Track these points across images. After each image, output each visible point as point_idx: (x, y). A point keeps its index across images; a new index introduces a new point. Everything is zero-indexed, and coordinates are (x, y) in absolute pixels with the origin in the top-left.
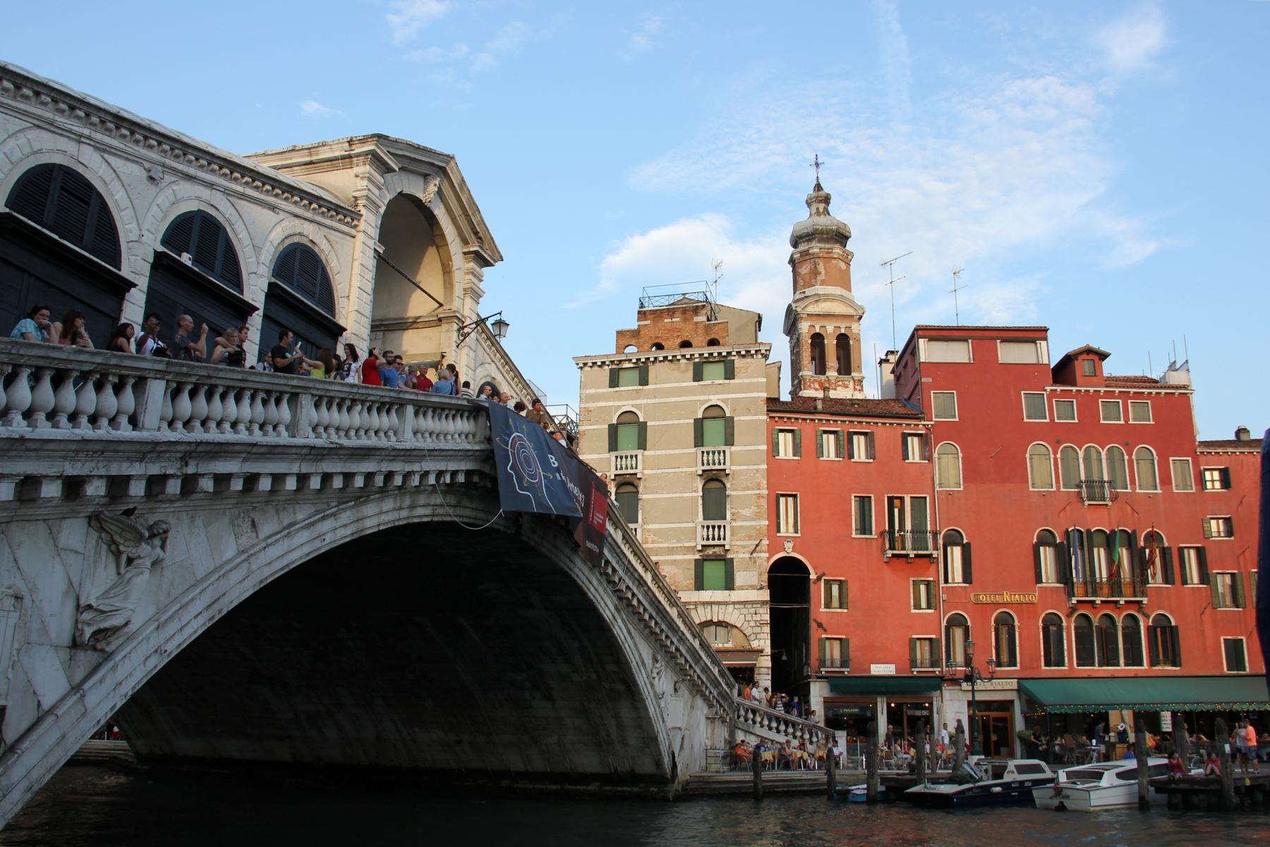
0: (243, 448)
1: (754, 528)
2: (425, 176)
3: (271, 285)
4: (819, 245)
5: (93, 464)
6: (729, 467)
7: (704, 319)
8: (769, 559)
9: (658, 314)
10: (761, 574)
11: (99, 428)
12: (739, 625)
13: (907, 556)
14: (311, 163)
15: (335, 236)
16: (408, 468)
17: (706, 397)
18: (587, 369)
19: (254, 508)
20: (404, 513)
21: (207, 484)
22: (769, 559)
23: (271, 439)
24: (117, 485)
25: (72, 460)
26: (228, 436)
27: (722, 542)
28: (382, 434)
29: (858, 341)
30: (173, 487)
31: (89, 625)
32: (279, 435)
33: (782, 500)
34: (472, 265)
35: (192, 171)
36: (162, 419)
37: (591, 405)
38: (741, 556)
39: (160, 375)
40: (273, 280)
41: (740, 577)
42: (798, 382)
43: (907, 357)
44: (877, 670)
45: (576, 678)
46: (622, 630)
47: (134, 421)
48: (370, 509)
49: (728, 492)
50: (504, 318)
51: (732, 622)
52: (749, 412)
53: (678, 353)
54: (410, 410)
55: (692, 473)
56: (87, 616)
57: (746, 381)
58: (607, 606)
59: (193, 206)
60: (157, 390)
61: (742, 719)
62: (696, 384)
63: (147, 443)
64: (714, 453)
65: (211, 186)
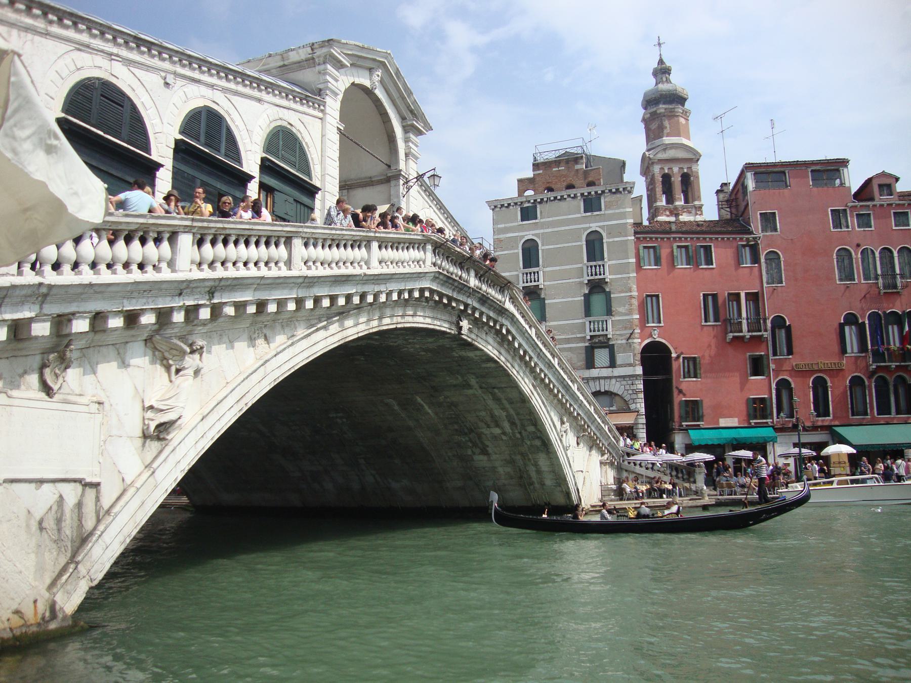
0: (253, 281)
1: (629, 321)
2: (371, 70)
3: (263, 159)
4: (663, 107)
5: (144, 300)
8: (640, 343)
9: (548, 165)
10: (634, 355)
11: (146, 272)
12: (620, 393)
13: (743, 337)
14: (284, 66)
15: (306, 119)
16: (377, 288)
17: (587, 225)
18: (497, 209)
19: (266, 326)
20: (375, 323)
21: (230, 311)
22: (640, 343)
23: (274, 272)
24: (164, 316)
25: (129, 298)
26: (242, 272)
27: (605, 332)
28: (356, 265)
29: (698, 177)
30: (205, 314)
31: (152, 420)
32: (280, 269)
33: (649, 299)
35: (196, 75)
36: (192, 262)
37: (502, 236)
38: (619, 342)
39: (188, 229)
40: (264, 155)
41: (620, 358)
42: (654, 212)
43: (739, 186)
44: (723, 422)
45: (504, 438)
46: (537, 401)
47: (171, 264)
48: (349, 323)
50: (438, 173)
51: (615, 391)
53: (565, 193)
54: (375, 245)
55: (581, 283)
56: (150, 414)
58: (526, 385)
59: (200, 103)
60: (186, 241)
61: (626, 463)
63: (183, 282)
65: (212, 86)
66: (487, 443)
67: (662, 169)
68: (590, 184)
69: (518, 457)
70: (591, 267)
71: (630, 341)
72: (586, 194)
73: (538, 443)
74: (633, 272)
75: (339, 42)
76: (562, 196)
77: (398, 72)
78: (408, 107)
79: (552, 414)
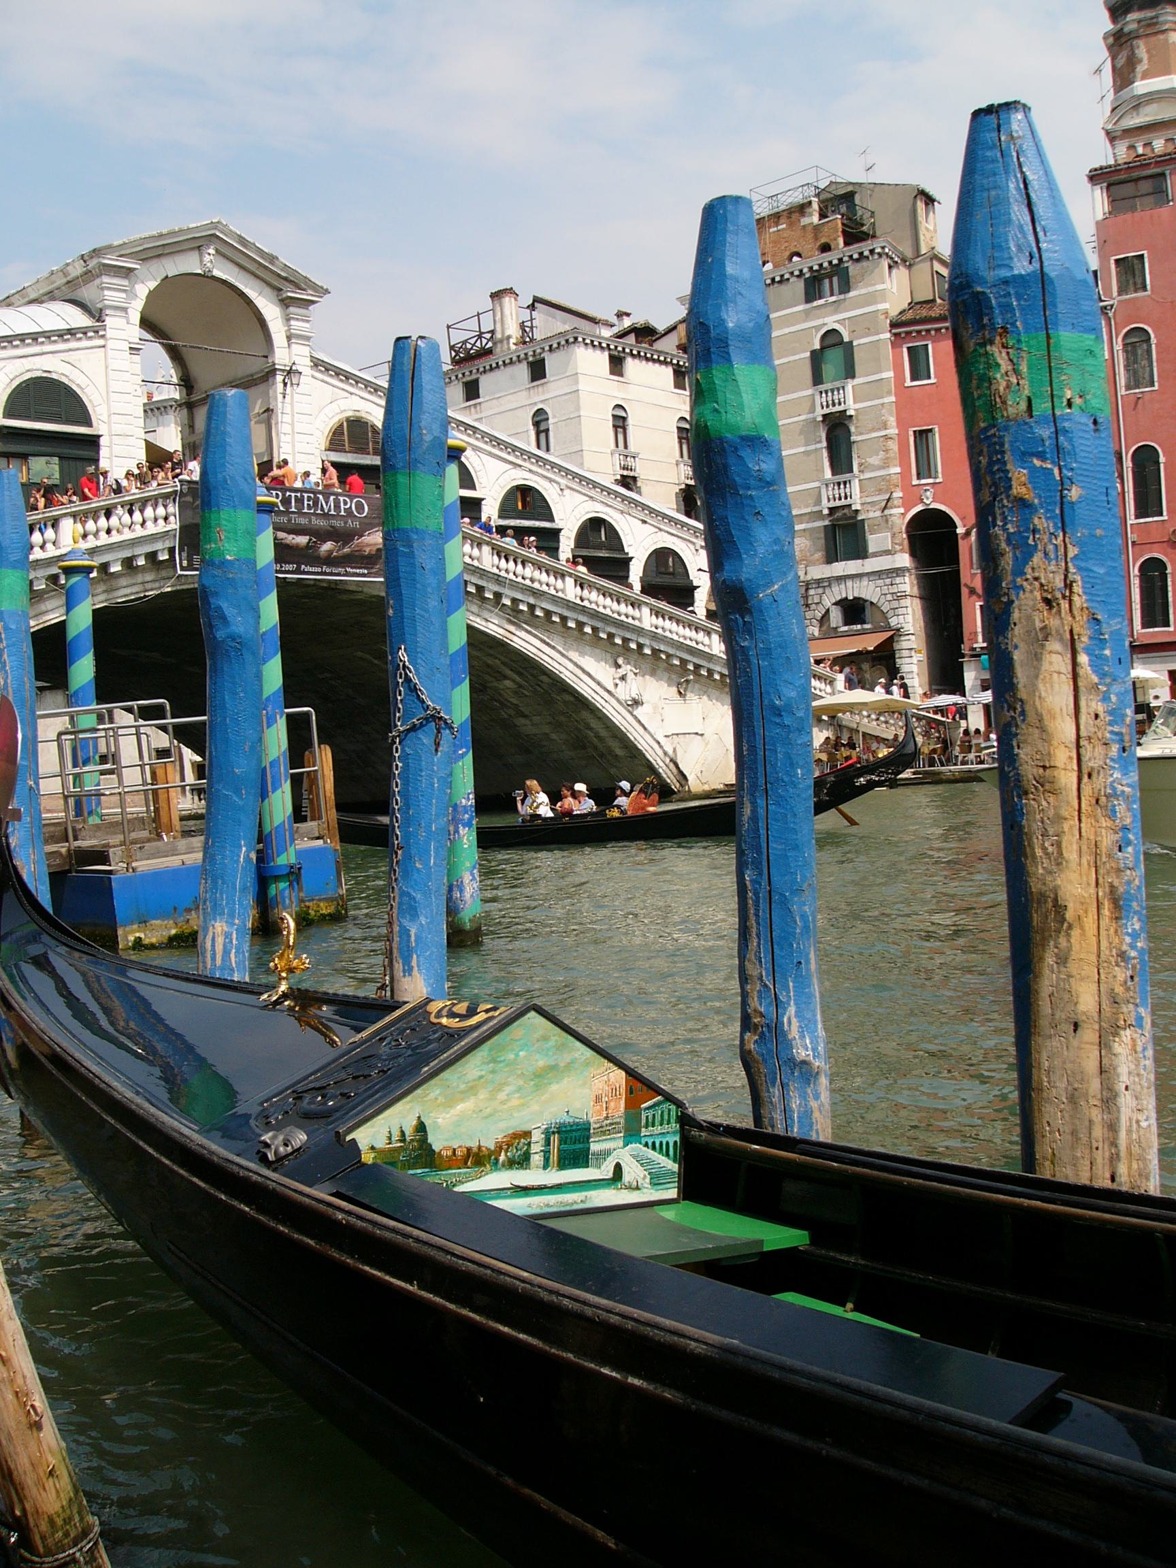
6: (851, 407)
7: (815, 219)
10: (893, 535)
14: (68, 282)
17: (820, 322)
27: (848, 501)
34: (292, 309)
38: (871, 515)
41: (874, 541)
49: (853, 438)
51: (868, 598)
52: (868, 332)
55: (814, 419)
57: (863, 291)
62: (808, 306)
64: (832, 391)
66: (514, 701)
67: (1132, 147)
68: (826, 248)
69: (562, 719)
70: (826, 392)
71: (886, 512)
72: (816, 267)
73: (568, 698)
74: (889, 393)
75: (110, 247)
76: (782, 276)
77: (242, 240)
78: (279, 275)
79: (574, 655)
